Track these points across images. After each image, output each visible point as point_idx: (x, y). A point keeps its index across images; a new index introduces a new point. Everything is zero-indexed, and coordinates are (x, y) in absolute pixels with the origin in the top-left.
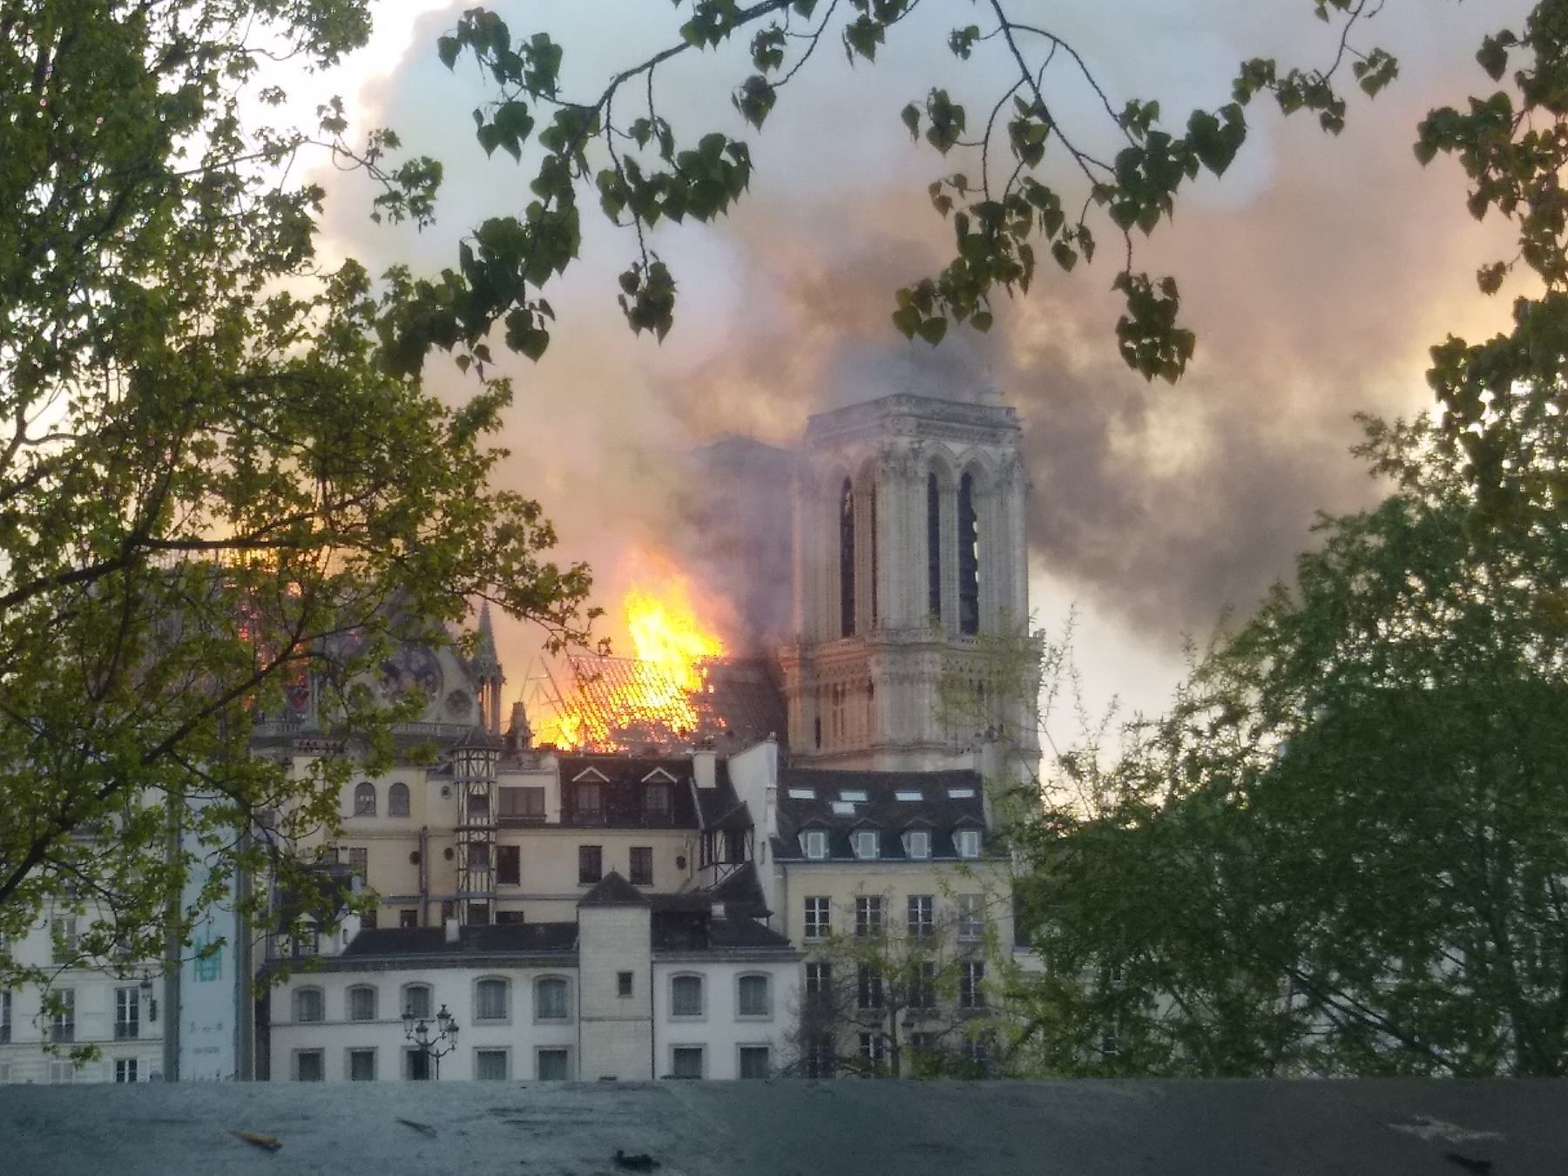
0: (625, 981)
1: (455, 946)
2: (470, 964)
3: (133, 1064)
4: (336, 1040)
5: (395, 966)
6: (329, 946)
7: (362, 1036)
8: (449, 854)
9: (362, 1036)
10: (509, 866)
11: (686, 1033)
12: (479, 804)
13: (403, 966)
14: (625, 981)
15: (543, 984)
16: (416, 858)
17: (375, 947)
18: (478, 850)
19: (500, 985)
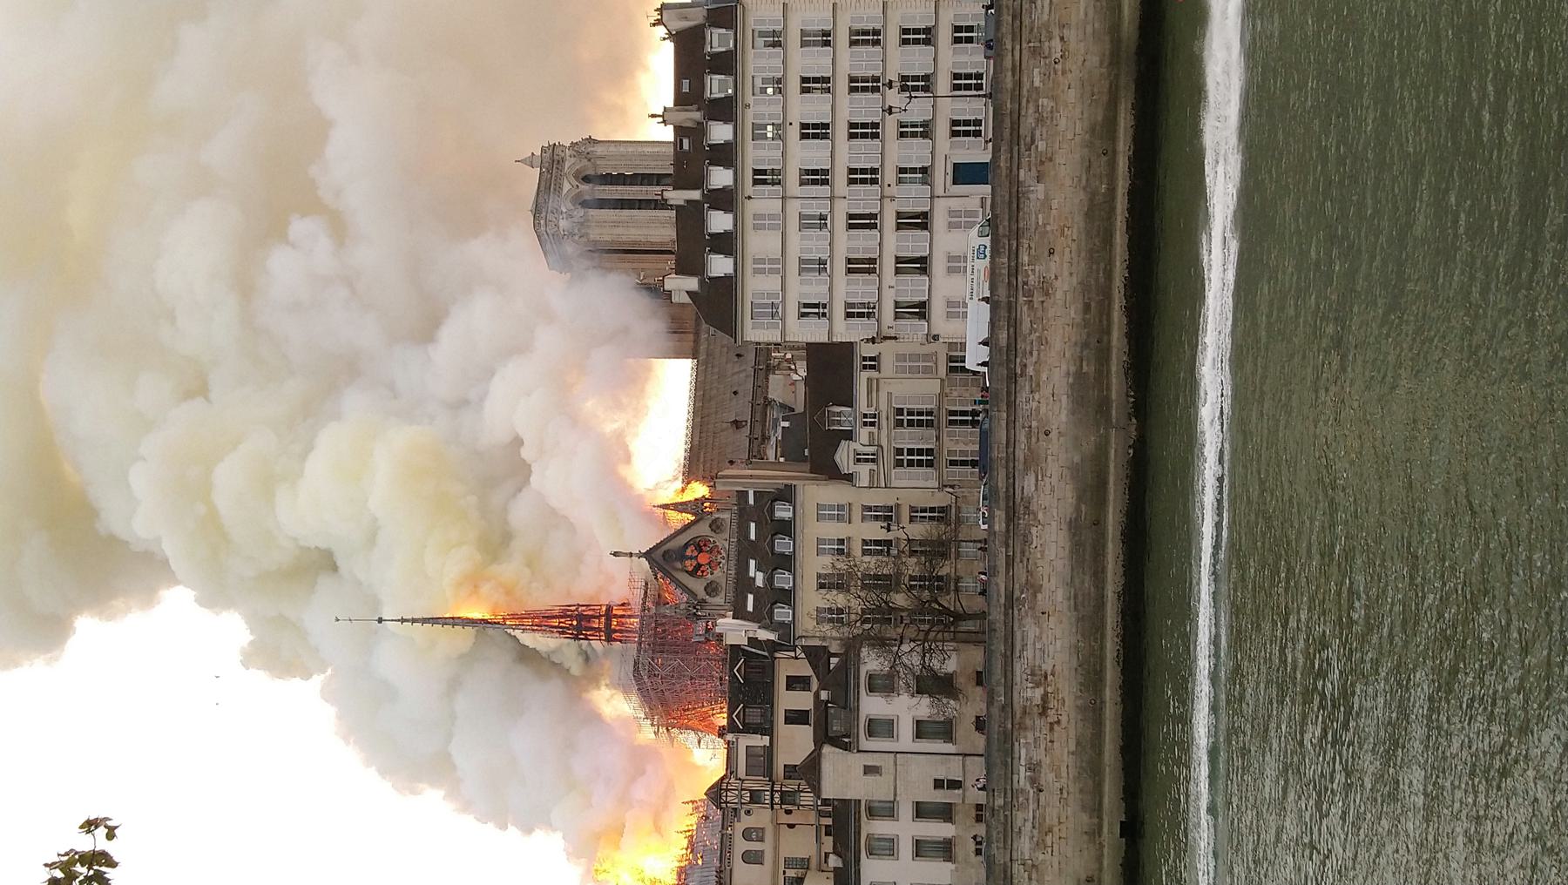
14: (869, 770)
15: (872, 813)
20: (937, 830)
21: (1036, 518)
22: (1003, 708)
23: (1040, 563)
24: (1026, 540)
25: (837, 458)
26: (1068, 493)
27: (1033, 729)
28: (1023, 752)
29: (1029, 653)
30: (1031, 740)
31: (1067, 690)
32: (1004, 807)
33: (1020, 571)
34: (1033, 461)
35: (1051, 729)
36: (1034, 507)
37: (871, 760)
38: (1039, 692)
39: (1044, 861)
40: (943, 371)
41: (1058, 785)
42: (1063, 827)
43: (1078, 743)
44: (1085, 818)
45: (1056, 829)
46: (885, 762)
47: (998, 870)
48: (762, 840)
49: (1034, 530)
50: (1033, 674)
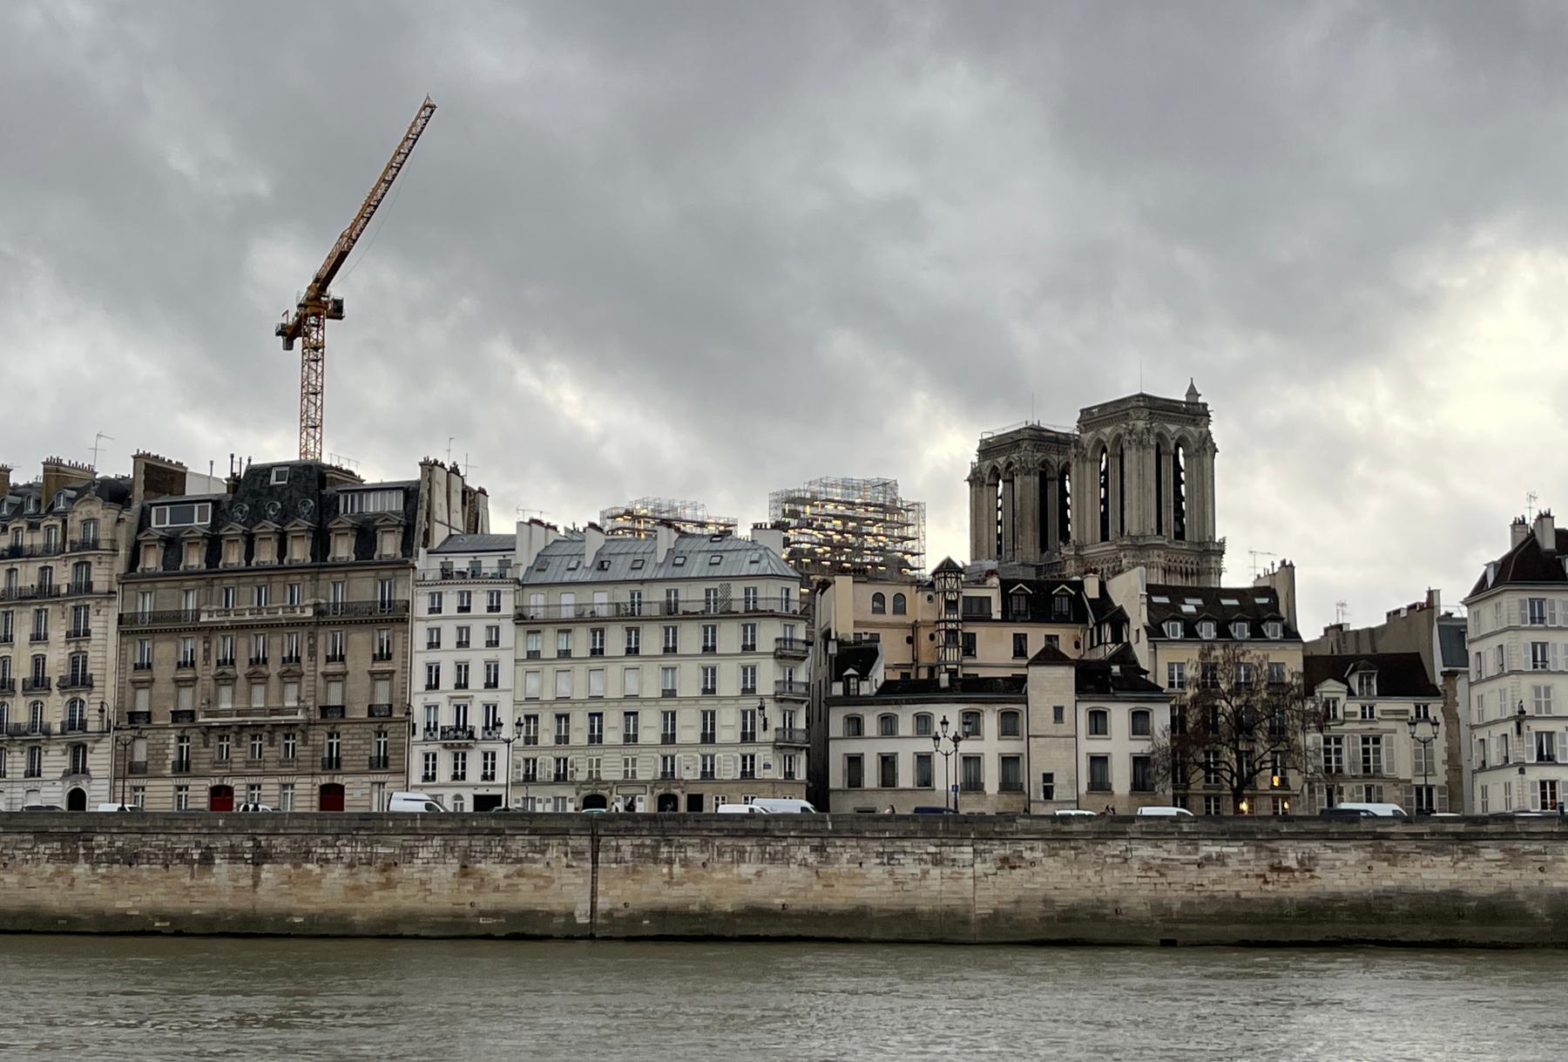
0: (1058, 713)
1: (945, 690)
2: (958, 701)
3: (752, 758)
4: (871, 750)
5: (908, 702)
6: (866, 689)
7: (888, 746)
8: (932, 637)
9: (888, 746)
10: (969, 647)
11: (1098, 746)
12: (950, 605)
13: (915, 702)
14: (1058, 713)
15: (1004, 715)
16: (910, 640)
17: (890, 693)
18: (951, 633)
19: (977, 715)
20: (991, 777)
21: (1459, 860)
22: (1277, 831)
23: (1417, 864)
24: (1438, 851)
25: (1331, 682)
26: (1487, 889)
27: (1258, 859)
28: (1235, 850)
29: (1329, 854)
30: (1246, 856)
31: (1297, 889)
32: (1180, 833)
33: (1410, 846)
34: (1514, 859)
35: (1258, 876)
36: (1470, 858)
37: (1067, 714)
38: (1294, 865)
39: (1130, 868)
40: (1420, 781)
41: (1205, 882)
42: (1166, 887)
43: (1248, 900)
44: (1177, 906)
45: (1163, 880)
46: (1066, 728)
47: (1120, 827)
48: (895, 612)
49: (1448, 858)
50: (1310, 859)
